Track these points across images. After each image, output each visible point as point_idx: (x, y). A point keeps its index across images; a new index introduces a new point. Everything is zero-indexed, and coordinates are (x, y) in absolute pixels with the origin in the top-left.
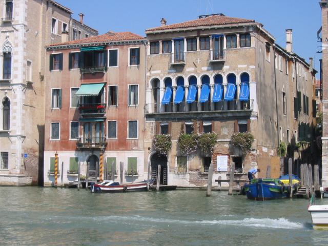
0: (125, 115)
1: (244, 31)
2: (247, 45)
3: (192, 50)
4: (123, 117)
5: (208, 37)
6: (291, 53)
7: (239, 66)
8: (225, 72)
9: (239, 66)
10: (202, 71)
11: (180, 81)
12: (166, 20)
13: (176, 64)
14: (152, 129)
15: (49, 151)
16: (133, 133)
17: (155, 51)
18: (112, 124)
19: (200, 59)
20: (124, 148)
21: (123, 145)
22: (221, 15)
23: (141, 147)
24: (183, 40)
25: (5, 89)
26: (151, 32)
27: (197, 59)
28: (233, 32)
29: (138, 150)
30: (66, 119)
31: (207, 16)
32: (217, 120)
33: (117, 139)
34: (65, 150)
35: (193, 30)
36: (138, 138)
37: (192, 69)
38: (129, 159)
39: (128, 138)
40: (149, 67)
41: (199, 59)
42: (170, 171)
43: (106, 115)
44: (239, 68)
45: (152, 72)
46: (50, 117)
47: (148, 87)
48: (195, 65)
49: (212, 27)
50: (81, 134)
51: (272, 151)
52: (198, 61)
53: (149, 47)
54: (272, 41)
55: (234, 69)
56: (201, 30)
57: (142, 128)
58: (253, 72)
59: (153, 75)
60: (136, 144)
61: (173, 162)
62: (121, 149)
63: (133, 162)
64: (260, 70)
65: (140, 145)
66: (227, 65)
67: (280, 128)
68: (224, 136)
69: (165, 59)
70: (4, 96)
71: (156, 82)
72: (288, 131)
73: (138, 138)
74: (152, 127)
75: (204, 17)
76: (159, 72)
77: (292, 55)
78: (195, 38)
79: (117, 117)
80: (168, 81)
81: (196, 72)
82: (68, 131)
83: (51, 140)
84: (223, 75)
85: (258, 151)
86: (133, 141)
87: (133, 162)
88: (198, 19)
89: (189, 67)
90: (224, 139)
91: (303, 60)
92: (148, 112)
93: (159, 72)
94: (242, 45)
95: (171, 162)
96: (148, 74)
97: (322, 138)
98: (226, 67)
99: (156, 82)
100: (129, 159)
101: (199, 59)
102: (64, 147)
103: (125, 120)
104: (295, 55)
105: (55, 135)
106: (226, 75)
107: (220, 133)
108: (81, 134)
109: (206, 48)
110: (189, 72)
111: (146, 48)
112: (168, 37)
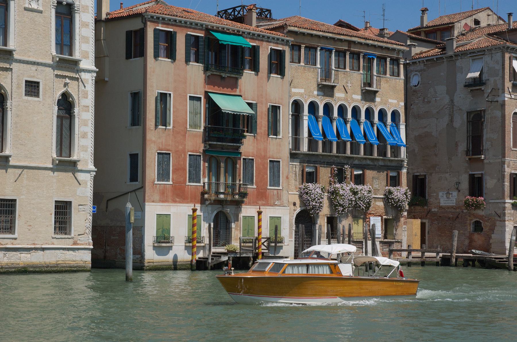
0: (265, 150)
5: (358, 54)
7: (390, 101)
9: (390, 101)
10: (354, 100)
11: (328, 108)
14: (296, 174)
15: (153, 202)
18: (249, 163)
20: (264, 202)
21: (263, 197)
23: (285, 202)
24: (316, 49)
25: (65, 77)
27: (347, 83)
30: (181, 147)
33: (255, 186)
34: (180, 202)
36: (281, 188)
43: (242, 149)
45: (294, 90)
46: (155, 142)
50: (204, 177)
52: (349, 85)
55: (385, 104)
56: (354, 42)
59: (295, 94)
60: (279, 198)
65: (284, 197)
69: (310, 74)
70: (63, 90)
73: (281, 188)
74: (295, 171)
76: (302, 91)
78: (344, 53)
79: (255, 153)
80: (313, 107)
81: (346, 99)
82: (185, 170)
83: (156, 182)
86: (275, 192)
93: (302, 91)
102: (178, 196)
105: (163, 175)
106: (378, 109)
108: (204, 177)
110: (340, 99)
112: (313, 43)
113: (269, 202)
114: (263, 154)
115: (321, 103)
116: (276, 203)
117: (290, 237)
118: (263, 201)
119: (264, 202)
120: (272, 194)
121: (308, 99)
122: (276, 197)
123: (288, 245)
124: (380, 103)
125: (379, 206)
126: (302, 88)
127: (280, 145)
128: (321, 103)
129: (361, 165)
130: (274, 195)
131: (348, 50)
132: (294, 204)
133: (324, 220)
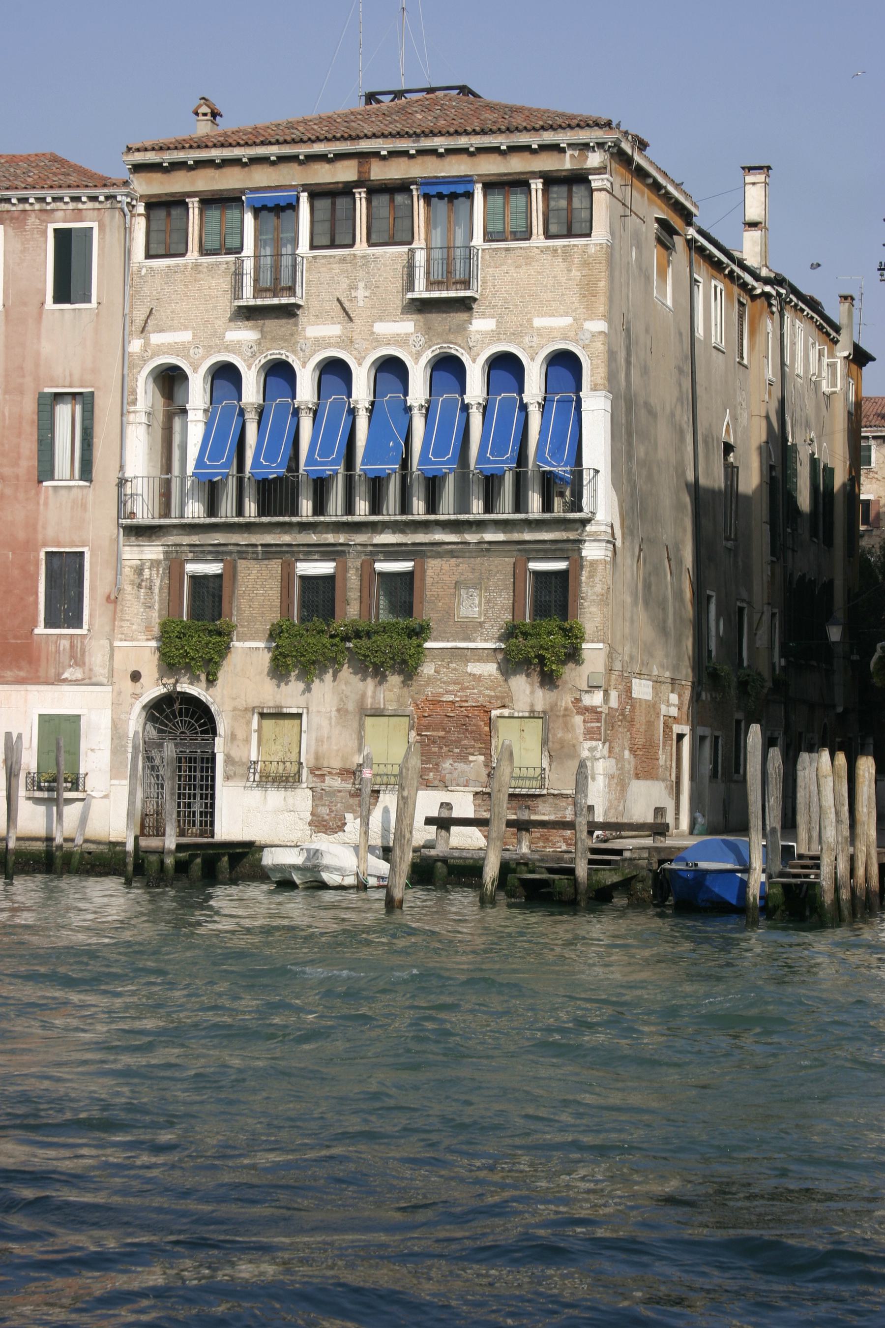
0: (32, 525)
1: (567, 163)
2: (576, 229)
3: (332, 245)
4: (21, 535)
5: (403, 187)
6: (764, 272)
7: (538, 322)
8: (479, 339)
9: (538, 322)
10: (378, 341)
12: (220, 108)
13: (259, 302)
16: (65, 605)
17: (167, 246)
19: (366, 287)
20: (22, 674)
22: (464, 90)
23: (100, 671)
26: (151, 157)
27: (353, 287)
28: (516, 165)
29: (88, 681)
31: (398, 94)
32: (439, 555)
35: (340, 156)
37: (334, 330)
38: (46, 721)
39: (40, 630)
40: (139, 315)
41: (361, 285)
42: (227, 778)
44: (540, 332)
45: (156, 339)
47: (134, 402)
48: (344, 309)
49: (427, 143)
51: (674, 698)
53: (140, 226)
54: (687, 217)
55: (516, 336)
56: (376, 154)
57: (105, 587)
58: (599, 346)
59: (160, 350)
60: (77, 657)
61: (241, 734)
62: (9, 674)
63: (61, 734)
64: (627, 343)
65: (97, 657)
66: (483, 315)
67: (709, 597)
68: (467, 630)
69: (214, 283)
71: (170, 379)
72: (741, 610)
75: (386, 99)
76: (185, 336)
77: (767, 281)
78: (346, 190)
81: (348, 342)
84: (465, 359)
85: (614, 695)
86: (65, 644)
87: (61, 734)
88: (360, 105)
89: (321, 317)
90: (467, 639)
91: (814, 305)
92: (132, 515)
93: (185, 336)
94: (553, 229)
95: (233, 737)
96: (136, 345)
97: (584, 646)
98: (481, 325)
99: (170, 379)
100: (46, 721)
101: (361, 285)
103: (30, 545)
104: (778, 281)
107: (449, 613)
109: (399, 235)
110: (320, 344)
111: (127, 231)
113: (42, 673)
114: (21, 535)
115: (249, 367)
116: (66, 675)
117: (115, 772)
118: (20, 668)
119: (22, 674)
120: (52, 648)
121: (204, 358)
122: (65, 658)
123: (106, 797)
124: (495, 335)
125: (478, 678)
126: (186, 328)
127: (84, 507)
128: (249, 367)
129: (406, 545)
130: (58, 651)
131: (358, 184)
132: (136, 676)
133: (249, 723)
